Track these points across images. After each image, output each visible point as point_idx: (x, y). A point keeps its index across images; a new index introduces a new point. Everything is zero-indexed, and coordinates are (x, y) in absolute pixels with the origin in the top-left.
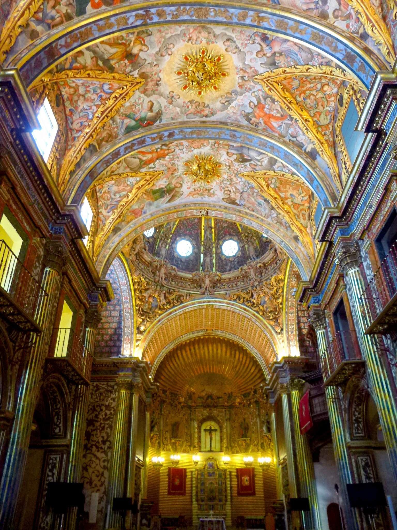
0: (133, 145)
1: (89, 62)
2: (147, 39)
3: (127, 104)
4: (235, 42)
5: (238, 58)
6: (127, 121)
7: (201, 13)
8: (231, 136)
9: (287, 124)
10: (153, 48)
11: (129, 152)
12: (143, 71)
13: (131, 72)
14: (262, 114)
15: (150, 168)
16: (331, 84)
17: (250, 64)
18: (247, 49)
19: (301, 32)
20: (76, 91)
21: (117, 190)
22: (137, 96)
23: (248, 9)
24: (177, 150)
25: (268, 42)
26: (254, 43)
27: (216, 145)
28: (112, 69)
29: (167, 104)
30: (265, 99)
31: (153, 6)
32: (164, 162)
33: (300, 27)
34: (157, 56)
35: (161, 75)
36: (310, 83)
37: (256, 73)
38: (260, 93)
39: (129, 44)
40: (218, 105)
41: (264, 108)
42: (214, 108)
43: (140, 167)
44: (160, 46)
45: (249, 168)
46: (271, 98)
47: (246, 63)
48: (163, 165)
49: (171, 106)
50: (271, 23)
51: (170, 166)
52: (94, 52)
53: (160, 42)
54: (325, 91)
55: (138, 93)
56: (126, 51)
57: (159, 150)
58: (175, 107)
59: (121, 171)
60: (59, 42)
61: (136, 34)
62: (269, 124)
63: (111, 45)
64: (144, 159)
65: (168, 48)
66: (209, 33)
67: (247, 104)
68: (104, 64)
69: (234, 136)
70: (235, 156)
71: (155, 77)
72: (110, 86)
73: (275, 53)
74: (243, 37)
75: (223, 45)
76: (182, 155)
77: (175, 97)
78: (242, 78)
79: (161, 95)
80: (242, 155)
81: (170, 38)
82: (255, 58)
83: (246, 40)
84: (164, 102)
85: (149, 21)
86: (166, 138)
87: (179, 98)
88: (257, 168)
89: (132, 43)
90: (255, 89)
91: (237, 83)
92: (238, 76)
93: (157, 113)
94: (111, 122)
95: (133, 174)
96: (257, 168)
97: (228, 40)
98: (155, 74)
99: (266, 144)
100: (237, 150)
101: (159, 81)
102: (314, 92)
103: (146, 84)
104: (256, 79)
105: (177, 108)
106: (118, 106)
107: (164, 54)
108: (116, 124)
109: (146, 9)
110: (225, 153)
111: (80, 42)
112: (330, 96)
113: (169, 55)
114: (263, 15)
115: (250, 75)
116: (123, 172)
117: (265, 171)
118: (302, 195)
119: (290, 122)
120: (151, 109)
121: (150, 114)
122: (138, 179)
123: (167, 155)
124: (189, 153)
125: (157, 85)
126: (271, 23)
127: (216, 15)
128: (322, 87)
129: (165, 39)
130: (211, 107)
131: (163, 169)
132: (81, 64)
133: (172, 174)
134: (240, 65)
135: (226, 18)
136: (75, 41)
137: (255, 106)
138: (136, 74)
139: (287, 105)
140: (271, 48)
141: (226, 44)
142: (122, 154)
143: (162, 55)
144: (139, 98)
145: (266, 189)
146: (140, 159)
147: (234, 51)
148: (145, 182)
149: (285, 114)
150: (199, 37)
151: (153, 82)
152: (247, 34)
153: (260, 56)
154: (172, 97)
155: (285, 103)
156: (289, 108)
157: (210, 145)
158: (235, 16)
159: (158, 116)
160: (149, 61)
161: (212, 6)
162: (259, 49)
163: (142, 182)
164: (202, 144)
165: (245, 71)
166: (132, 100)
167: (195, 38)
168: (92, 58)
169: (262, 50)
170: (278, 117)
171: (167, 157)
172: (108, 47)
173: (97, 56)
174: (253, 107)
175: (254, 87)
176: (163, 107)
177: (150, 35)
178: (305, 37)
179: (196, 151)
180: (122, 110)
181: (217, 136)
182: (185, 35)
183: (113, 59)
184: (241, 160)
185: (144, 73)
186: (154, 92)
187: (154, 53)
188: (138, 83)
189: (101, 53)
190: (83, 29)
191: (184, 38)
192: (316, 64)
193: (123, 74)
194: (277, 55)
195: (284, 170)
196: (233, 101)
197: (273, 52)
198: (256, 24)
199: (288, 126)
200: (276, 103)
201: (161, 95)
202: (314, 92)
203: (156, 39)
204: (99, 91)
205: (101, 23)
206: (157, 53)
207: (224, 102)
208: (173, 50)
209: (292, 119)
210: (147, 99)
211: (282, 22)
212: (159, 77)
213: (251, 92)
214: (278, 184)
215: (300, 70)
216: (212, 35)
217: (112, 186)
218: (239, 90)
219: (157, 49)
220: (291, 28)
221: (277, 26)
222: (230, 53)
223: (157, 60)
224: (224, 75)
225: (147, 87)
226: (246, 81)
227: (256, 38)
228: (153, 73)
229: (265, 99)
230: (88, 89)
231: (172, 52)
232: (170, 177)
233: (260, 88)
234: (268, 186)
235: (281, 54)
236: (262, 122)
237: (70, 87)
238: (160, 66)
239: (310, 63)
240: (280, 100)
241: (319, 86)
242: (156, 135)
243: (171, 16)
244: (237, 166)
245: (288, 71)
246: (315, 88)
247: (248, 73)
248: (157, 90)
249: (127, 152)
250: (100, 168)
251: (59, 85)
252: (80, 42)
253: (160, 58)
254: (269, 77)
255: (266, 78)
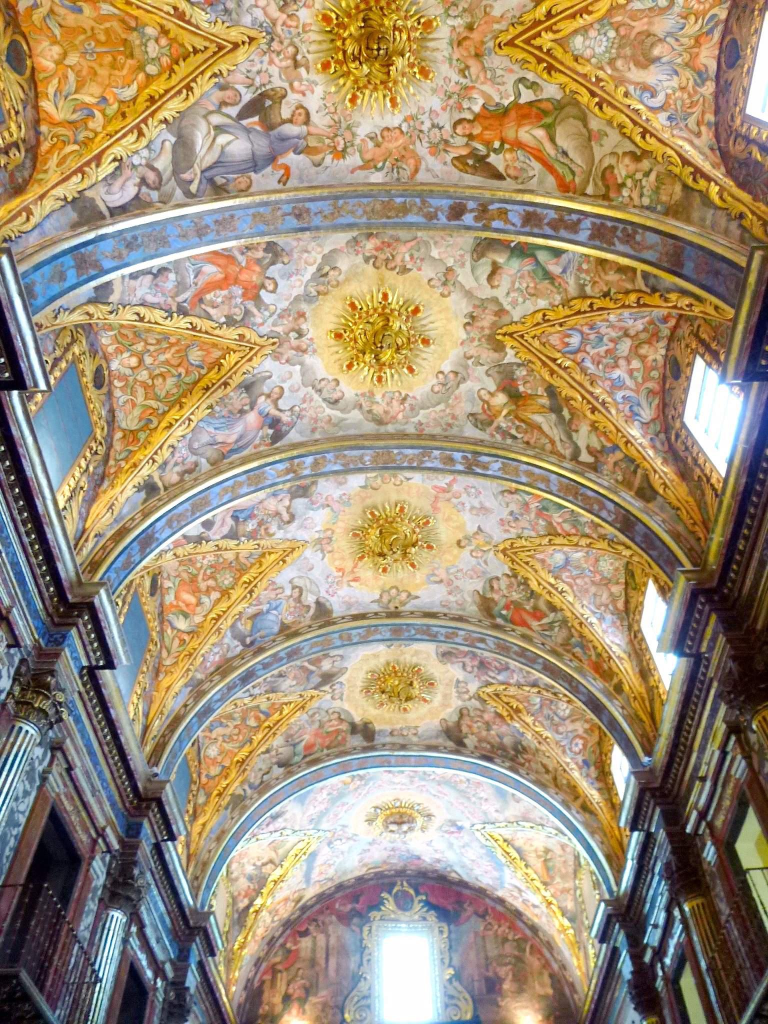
0: (556, 225)
1: (584, 429)
2: (478, 409)
3: (542, 303)
4: (324, 400)
5: (314, 373)
6: (555, 269)
7: (386, 457)
8: (308, 211)
9: (185, 289)
10: (470, 390)
11: (571, 211)
12: (496, 355)
13: (519, 365)
14: (244, 277)
15: (533, 86)
16: (128, 372)
17: (291, 368)
18: (301, 394)
19: (226, 490)
20: (638, 346)
21: (657, 19)
22: (518, 308)
23: (312, 476)
24: (448, 127)
25: (269, 421)
26: (291, 409)
27: (340, 148)
28: (551, 391)
29: (459, 270)
30: (247, 313)
31: (460, 472)
32: (487, 88)
33: (230, 494)
34: (464, 373)
35: (464, 336)
36: (167, 362)
37: (277, 356)
38: (259, 320)
39: (509, 414)
40: (344, 263)
41: (244, 295)
42: (353, 257)
43: (559, 106)
44: (457, 392)
45: (238, 80)
46: (236, 322)
47: (298, 367)
48: (493, 80)
49: (450, 262)
50: (273, 472)
51: (475, 69)
52: (570, 437)
53: (456, 398)
54: (131, 356)
55: (516, 315)
56: (518, 406)
57: (497, 144)
58: (441, 260)
59: (614, 136)
60: (610, 519)
61: (495, 425)
62: (222, 261)
63: (540, 428)
64: (540, 133)
65: (444, 385)
66: (370, 412)
67: (281, 283)
68: (561, 410)
69: (298, 216)
70: (286, 112)
71: (475, 334)
72: (567, 340)
73: (252, 409)
74: (311, 413)
75: (344, 390)
76: (436, 103)
77: (438, 284)
78: (300, 334)
79: (468, 294)
80: (269, 126)
81: (439, 404)
82: (284, 381)
83: (305, 409)
84: (464, 276)
85: (469, 456)
86: (471, 205)
87: (430, 280)
88: (218, 95)
89: (504, 412)
90: (271, 320)
91: (310, 319)
92: (309, 336)
93: (481, 255)
94: (588, 289)
95: (584, 98)
96: (218, 95)
97: (336, 401)
98: (472, 340)
99: (218, 232)
100: (283, 139)
101: (468, 324)
102: (152, 348)
103: (494, 326)
104: (274, 344)
105: (437, 257)
106: (564, 312)
107: (451, 376)
108: (578, 278)
109: (469, 471)
110: (315, 118)
111: (583, 490)
112: (119, 351)
113: (442, 372)
114: (288, 477)
115: (286, 345)
116: (608, 130)
117: (192, 100)
118: (44, 10)
119: (180, 299)
120: (495, 269)
121: (501, 259)
122: (578, 41)
123: (477, 117)
124: (414, 111)
125: (473, 318)
126: (273, 472)
127: (361, 458)
128: (141, 361)
129: (446, 402)
130: (360, 256)
131: (497, 61)
132: (598, 437)
133: (470, 28)
134: (308, 359)
135: (345, 456)
136: (589, 498)
137: (263, 286)
138: (510, 357)
139: (200, 331)
140: (260, 413)
141: (339, 394)
142: (587, 223)
143: (456, 373)
144: (514, 303)
145: (169, 26)
146: (552, 140)
147: (323, 383)
148: (561, 26)
149: (197, 310)
150: (388, 404)
151: (480, 324)
152: (305, 421)
153: (277, 390)
154: (444, 284)
155: (207, 333)
156: (194, 329)
157: (357, 141)
158: (330, 461)
159: (482, 248)
160: (481, 370)
161: (367, 469)
162: (281, 403)
163: (567, 27)
164: (378, 145)
165: (298, 349)
166: (529, 307)
167: (395, 403)
168: (577, 431)
169: (275, 403)
170: (209, 292)
171: (477, 109)
172: (546, 428)
173: (569, 428)
174: (267, 282)
175: (274, 324)
176: (468, 265)
177: (472, 415)
178: (217, 489)
179: (395, 120)
180: (557, 299)
181: (341, 202)
182: (412, 408)
183: (543, 406)
184: (268, 103)
185: (495, 351)
186: (482, 304)
187: (469, 382)
188: (511, 335)
189: (560, 427)
190: (570, 498)
191: (414, 402)
192: (180, 445)
193: (533, 370)
194: (247, 408)
195: (145, 153)
196: (314, 278)
197: (256, 407)
198: (296, 461)
199: (181, 286)
200: (223, 320)
201: (468, 294)
202: (152, 348)
203: (462, 405)
204: (592, 337)
205: (543, 486)
206: (464, 380)
207: (331, 273)
208: (435, 381)
209: (183, 312)
210: (500, 293)
211: (257, 484)
212: (468, 333)
213: (279, 311)
214: (136, 41)
215: (201, 409)
216: (366, 407)
217: (670, 34)
218: (304, 307)
219: (461, 386)
220: (241, 484)
221: (263, 473)
222: (330, 378)
223: (466, 367)
224: (338, 336)
225: (495, 318)
226: (293, 330)
227: (289, 419)
228: (476, 343)
229: (247, 313)
230: (611, 345)
231: (437, 377)
232: (480, 13)
233: (261, 328)
234: (164, 31)
235: (242, 412)
236: (240, 258)
237: (643, 358)
238: (462, 354)
239: (190, 436)
240: (217, 332)
241: (148, 360)
242: (496, 224)
243: (433, 455)
244: (274, 70)
245: (220, 391)
246: (155, 354)
247: (292, 348)
248: (475, 306)
249: (574, 217)
250: (650, 248)
251: (662, 371)
252: (583, 490)
253: (460, 370)
254: (250, 360)
255: (256, 354)
